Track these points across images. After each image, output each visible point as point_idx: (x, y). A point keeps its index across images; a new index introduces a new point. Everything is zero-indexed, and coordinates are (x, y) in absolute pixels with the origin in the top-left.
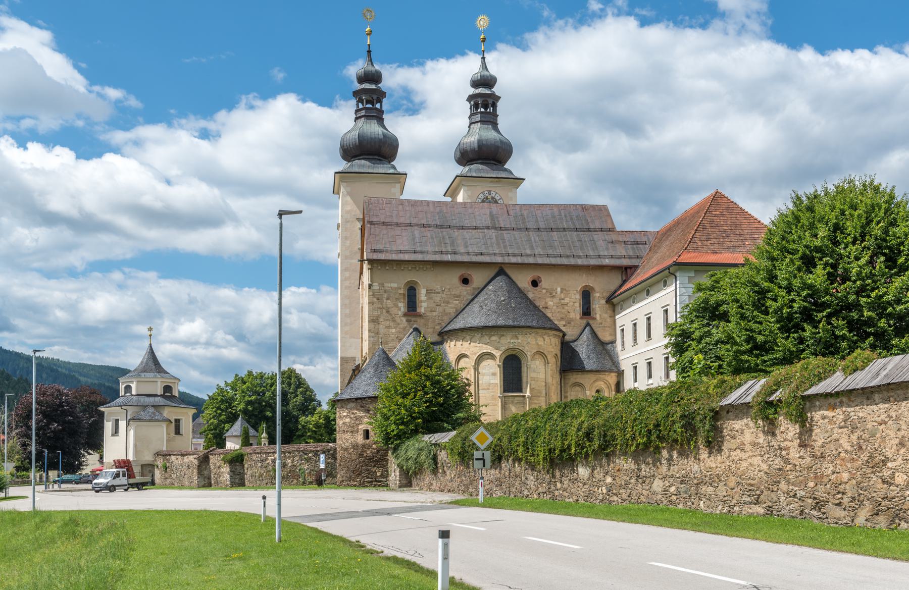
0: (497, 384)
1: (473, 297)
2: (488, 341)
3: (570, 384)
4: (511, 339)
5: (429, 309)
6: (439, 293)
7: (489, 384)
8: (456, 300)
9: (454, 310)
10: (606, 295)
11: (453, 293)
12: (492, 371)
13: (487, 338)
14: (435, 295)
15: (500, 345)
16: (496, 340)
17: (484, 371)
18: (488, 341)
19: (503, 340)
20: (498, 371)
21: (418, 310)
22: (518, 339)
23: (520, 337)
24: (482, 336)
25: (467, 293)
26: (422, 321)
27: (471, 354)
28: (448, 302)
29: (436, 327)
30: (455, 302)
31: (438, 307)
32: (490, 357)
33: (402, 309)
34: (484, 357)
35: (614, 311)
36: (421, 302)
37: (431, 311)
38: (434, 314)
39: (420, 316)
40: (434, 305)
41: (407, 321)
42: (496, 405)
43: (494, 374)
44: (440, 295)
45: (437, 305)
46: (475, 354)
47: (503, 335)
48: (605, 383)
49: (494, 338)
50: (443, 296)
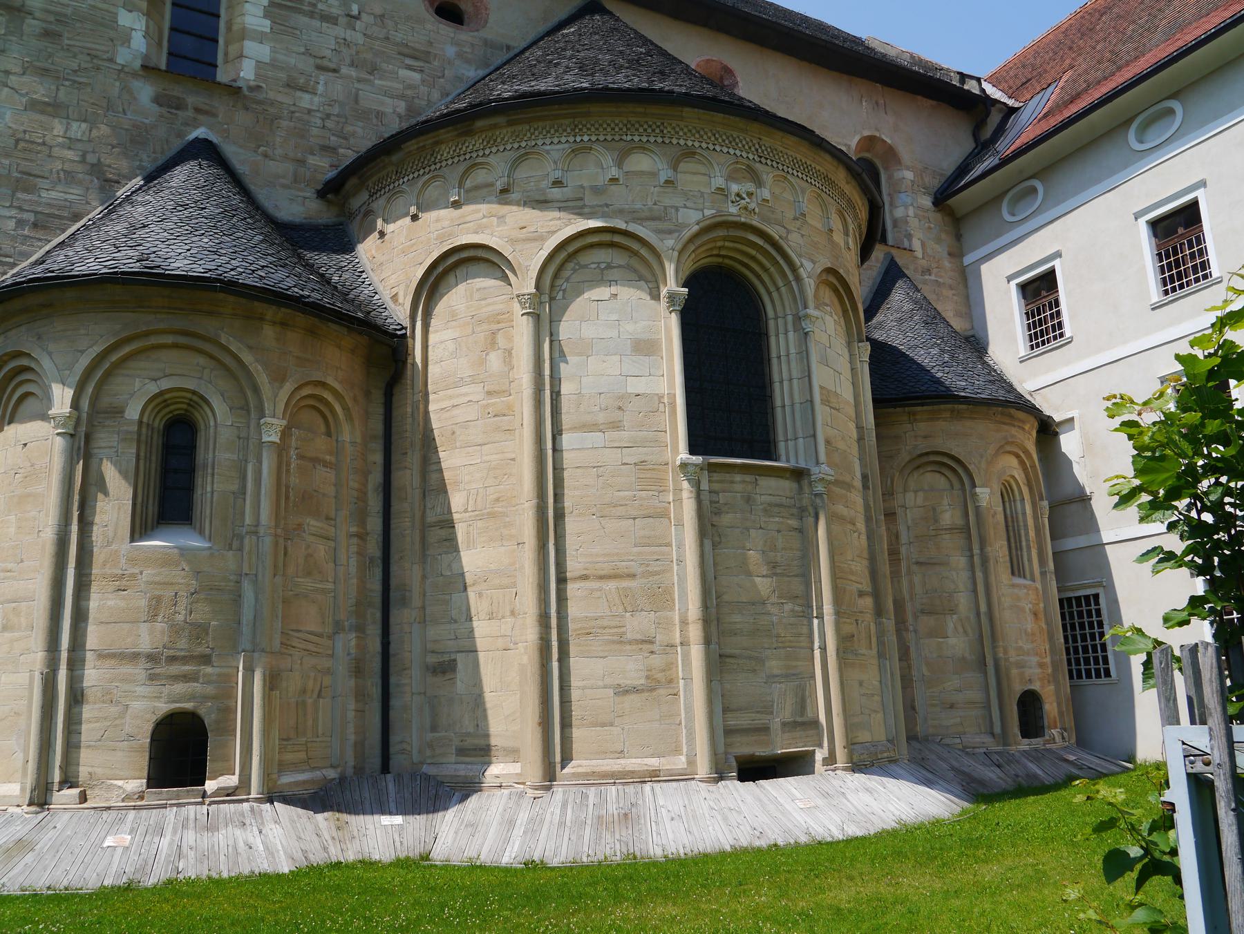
0: (657, 401)
1: (481, 73)
2: (614, 172)
3: (905, 456)
4: (730, 178)
5: (283, 75)
6: (331, 19)
7: (621, 402)
8: (410, 68)
9: (401, 107)
10: (935, 183)
11: (399, 37)
12: (632, 329)
13: (608, 159)
14: (316, 23)
15: (678, 201)
16: (654, 174)
17: (589, 331)
18: (614, 172)
19: (692, 178)
20: (669, 330)
21: (222, 76)
22: (759, 183)
23: (768, 176)
24: (580, 150)
25: (460, 55)
26: (242, 119)
27: (513, 241)
28: (373, 70)
29: (313, 160)
30: (403, 73)
31: (323, 78)
32: (618, 258)
33: (139, 42)
34: (586, 258)
35: (958, 237)
36: (244, 34)
37: (291, 85)
38: (305, 101)
39: (233, 91)
40: (306, 65)
41: (157, 100)
42: (664, 515)
43: (645, 347)
44: (339, 31)
45: (320, 68)
46: (541, 239)
47: (689, 154)
48: (1022, 463)
49: (641, 162)
50: (349, 34)
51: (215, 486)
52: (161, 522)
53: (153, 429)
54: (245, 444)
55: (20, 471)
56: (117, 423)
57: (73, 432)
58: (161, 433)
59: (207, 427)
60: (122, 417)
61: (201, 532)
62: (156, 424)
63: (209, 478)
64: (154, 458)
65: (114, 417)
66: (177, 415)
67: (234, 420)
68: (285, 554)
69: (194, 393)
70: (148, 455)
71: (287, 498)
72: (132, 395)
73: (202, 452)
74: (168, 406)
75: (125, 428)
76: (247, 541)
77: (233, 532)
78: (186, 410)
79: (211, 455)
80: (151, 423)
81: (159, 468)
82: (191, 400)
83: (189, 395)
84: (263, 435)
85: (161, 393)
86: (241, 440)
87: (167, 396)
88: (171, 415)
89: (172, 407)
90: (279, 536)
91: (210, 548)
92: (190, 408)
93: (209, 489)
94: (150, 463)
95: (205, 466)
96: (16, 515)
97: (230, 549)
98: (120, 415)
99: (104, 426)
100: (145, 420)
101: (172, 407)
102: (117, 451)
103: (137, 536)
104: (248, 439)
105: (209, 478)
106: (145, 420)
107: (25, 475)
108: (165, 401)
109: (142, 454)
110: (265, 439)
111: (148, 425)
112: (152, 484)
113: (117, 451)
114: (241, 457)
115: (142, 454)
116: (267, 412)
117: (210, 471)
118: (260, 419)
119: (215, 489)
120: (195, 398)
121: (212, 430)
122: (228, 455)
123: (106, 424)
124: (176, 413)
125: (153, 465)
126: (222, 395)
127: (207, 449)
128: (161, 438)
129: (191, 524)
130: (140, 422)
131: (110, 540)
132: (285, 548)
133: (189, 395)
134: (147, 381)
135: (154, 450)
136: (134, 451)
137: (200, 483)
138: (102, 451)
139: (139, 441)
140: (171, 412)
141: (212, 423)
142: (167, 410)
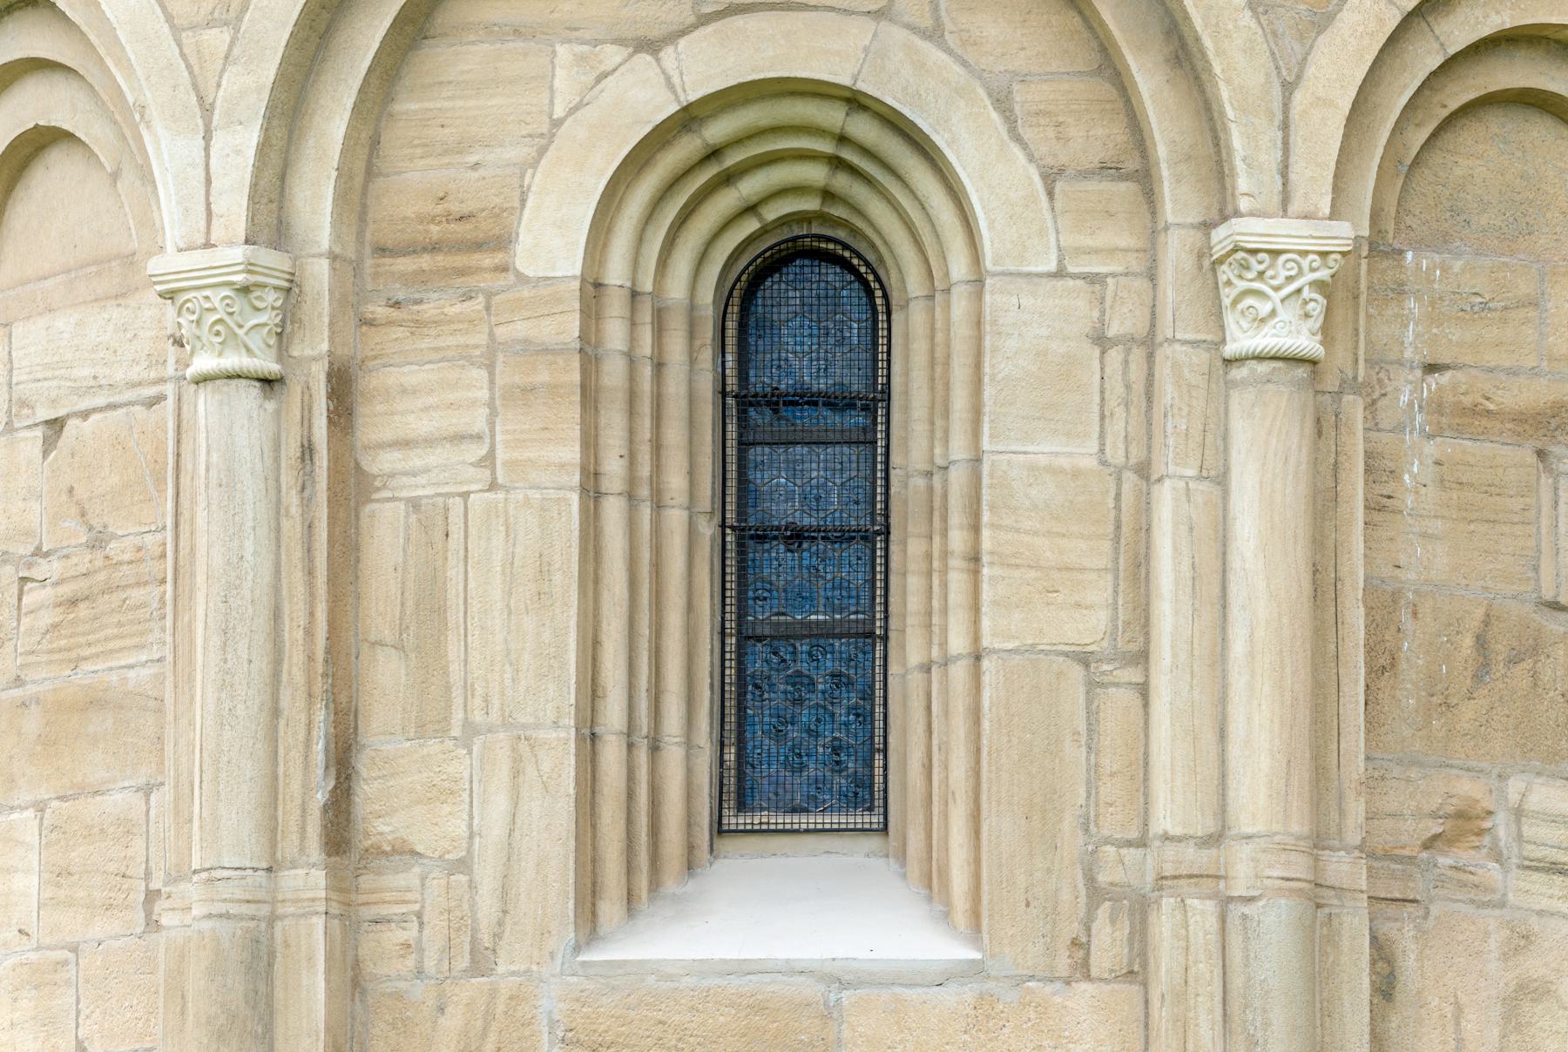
51: (986, 623)
52: (732, 820)
53: (659, 317)
54: (1137, 373)
55: (42, 569)
56: (478, 303)
57: (271, 367)
58: (708, 332)
59: (936, 290)
60: (503, 269)
61: (932, 882)
62: (676, 289)
63: (958, 580)
64: (676, 481)
65: (463, 272)
66: (784, 221)
67: (1068, 240)
68: (1385, 988)
69: (855, 101)
70: (645, 470)
71: (1382, 665)
72: (544, 143)
73: (920, 429)
74: (728, 179)
75: (520, 329)
76: (1164, 923)
77: (1090, 880)
78: (828, 195)
79: (959, 448)
80: (647, 285)
81: (708, 530)
82: (843, 139)
83: (833, 116)
84: (1230, 319)
85: (689, 118)
86: (1115, 356)
87: (718, 130)
88: (751, 226)
89: (751, 186)
90: (1339, 890)
91: (974, 971)
92: (842, 182)
93: (958, 643)
94: (658, 506)
95: (935, 509)
96: (40, 807)
97: (1083, 970)
98: (487, 260)
99: (419, 324)
100: (616, 273)
101: (751, 186)
102: (489, 460)
103: (610, 909)
104: (1149, 343)
105: (958, 580)
106: (616, 273)
107: (66, 590)
108: (714, 154)
109: (613, 467)
110: (1242, 340)
111: (634, 294)
112: (674, 620)
113: (489, 460)
114: (1116, 455)
115: (613, 467)
116: (1243, 183)
117: (958, 539)
118: (1207, 226)
119: (986, 642)
120: (864, 129)
121: (960, 306)
122: (1047, 448)
123: (429, 310)
124: (772, 213)
125: (676, 519)
126: (1003, 103)
127: (940, 408)
128: (706, 356)
129: (885, 829)
130: (593, 289)
131: (486, 940)
132: (1382, 952)
133: (833, 116)
134: (612, 55)
135: (675, 434)
136: (571, 453)
137: (914, 603)
138: (416, 459)
139: (590, 397)
140: (751, 209)
141: (959, 267)
142: (726, 201)
